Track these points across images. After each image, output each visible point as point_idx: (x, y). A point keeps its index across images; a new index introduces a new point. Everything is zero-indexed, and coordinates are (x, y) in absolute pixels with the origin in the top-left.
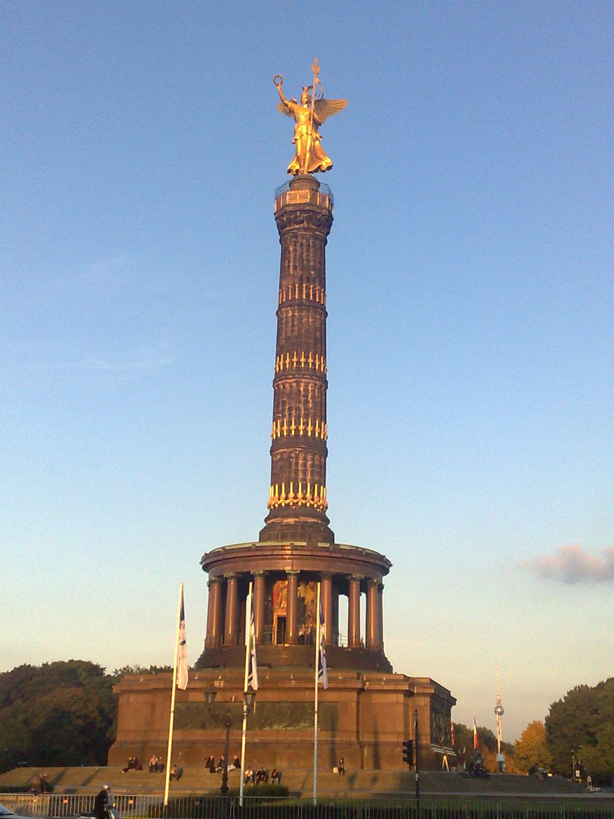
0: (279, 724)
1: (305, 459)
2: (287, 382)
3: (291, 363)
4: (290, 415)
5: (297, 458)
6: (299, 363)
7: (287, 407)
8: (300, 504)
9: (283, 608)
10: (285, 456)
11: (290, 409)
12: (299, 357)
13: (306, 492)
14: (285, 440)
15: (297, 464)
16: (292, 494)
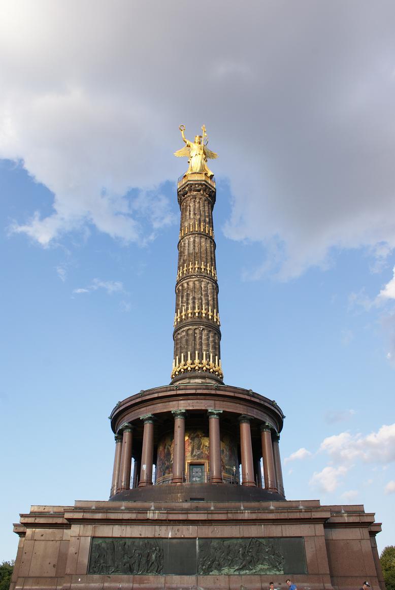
0: (230, 566)
1: (208, 335)
2: (190, 281)
3: (193, 269)
4: (194, 303)
5: (201, 334)
6: (200, 268)
7: (191, 297)
8: (204, 368)
9: (195, 456)
10: (190, 332)
11: (194, 298)
12: (200, 264)
13: (210, 361)
14: (190, 320)
15: (201, 338)
16: (197, 361)
